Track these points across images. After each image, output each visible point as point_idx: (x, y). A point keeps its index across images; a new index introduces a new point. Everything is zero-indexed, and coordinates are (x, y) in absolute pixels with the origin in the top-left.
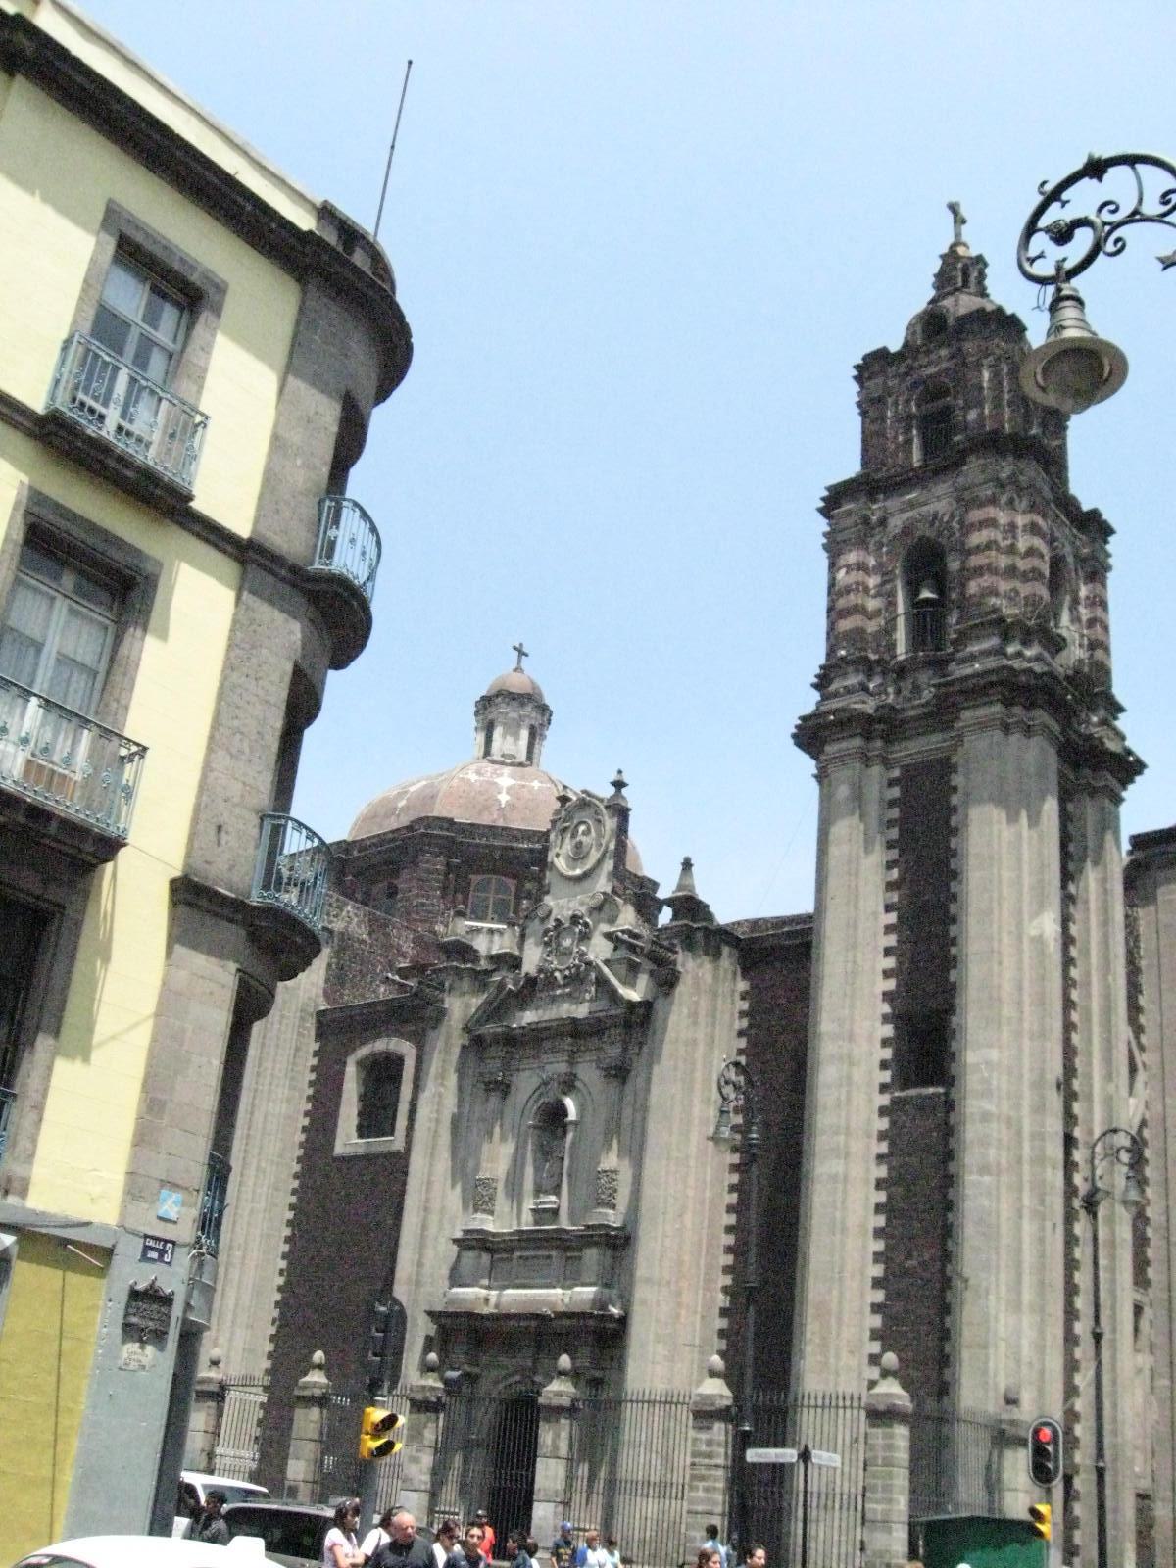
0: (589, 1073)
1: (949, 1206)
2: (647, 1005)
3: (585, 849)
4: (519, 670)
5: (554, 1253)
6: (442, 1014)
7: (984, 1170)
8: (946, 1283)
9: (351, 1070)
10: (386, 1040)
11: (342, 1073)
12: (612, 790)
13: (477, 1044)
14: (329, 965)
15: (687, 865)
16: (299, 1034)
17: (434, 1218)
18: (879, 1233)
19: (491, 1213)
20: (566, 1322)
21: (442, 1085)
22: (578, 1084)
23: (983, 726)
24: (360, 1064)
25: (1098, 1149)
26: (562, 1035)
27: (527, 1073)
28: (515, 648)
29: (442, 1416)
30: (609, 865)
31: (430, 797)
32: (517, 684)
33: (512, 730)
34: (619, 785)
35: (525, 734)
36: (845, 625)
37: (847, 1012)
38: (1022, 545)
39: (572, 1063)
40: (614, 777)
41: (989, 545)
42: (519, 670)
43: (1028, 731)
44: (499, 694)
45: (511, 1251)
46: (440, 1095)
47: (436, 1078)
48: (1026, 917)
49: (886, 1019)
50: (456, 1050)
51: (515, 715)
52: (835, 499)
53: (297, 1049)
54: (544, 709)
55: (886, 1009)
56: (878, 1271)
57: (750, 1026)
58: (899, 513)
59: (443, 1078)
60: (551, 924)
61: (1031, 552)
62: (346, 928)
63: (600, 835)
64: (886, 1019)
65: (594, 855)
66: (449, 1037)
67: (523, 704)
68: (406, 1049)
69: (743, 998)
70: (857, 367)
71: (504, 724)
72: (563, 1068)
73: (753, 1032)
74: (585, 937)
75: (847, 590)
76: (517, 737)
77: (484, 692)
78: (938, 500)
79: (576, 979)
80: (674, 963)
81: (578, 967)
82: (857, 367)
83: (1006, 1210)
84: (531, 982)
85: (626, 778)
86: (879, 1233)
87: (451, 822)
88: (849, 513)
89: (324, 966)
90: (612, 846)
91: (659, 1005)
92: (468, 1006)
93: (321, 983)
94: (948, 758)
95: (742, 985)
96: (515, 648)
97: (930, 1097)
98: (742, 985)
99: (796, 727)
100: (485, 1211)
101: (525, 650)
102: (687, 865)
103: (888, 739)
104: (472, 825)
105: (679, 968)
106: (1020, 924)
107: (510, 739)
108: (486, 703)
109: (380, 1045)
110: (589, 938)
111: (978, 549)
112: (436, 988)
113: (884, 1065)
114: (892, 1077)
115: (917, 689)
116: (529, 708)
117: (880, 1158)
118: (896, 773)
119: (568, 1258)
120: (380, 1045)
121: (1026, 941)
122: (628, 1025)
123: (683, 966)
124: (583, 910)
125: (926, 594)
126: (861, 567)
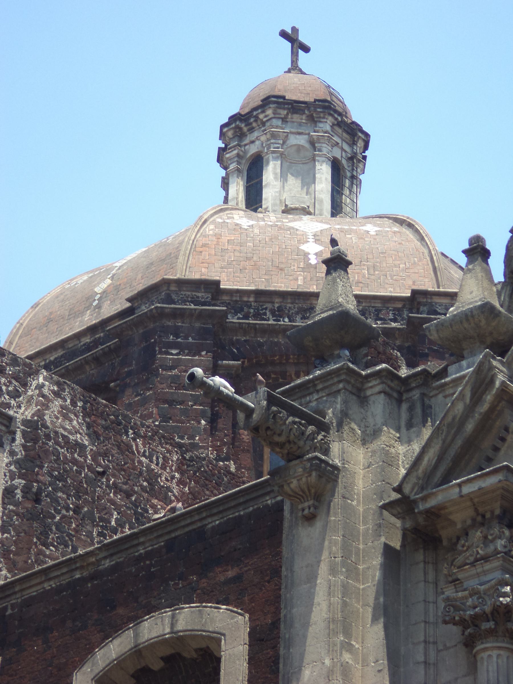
4: (295, 67)
6: (329, 475)
10: (168, 613)
21: (348, 647)
28: (284, 34)
31: (169, 254)
32: (295, 89)
33: (299, 166)
35: (324, 173)
42: (295, 67)
44: (266, 102)
47: (331, 633)
50: (373, 565)
51: (302, 141)
54: (355, 135)
59: (347, 632)
62: (40, 414)
66: (350, 535)
67: (313, 120)
68: (230, 628)
71: (282, 156)
76: (309, 180)
77: (235, 110)
87: (212, 287)
92: (389, 461)
96: (284, 34)
101: (302, 38)
104: (259, 293)
107: (294, 183)
108: (238, 127)
112: (311, 420)
116: (326, 125)
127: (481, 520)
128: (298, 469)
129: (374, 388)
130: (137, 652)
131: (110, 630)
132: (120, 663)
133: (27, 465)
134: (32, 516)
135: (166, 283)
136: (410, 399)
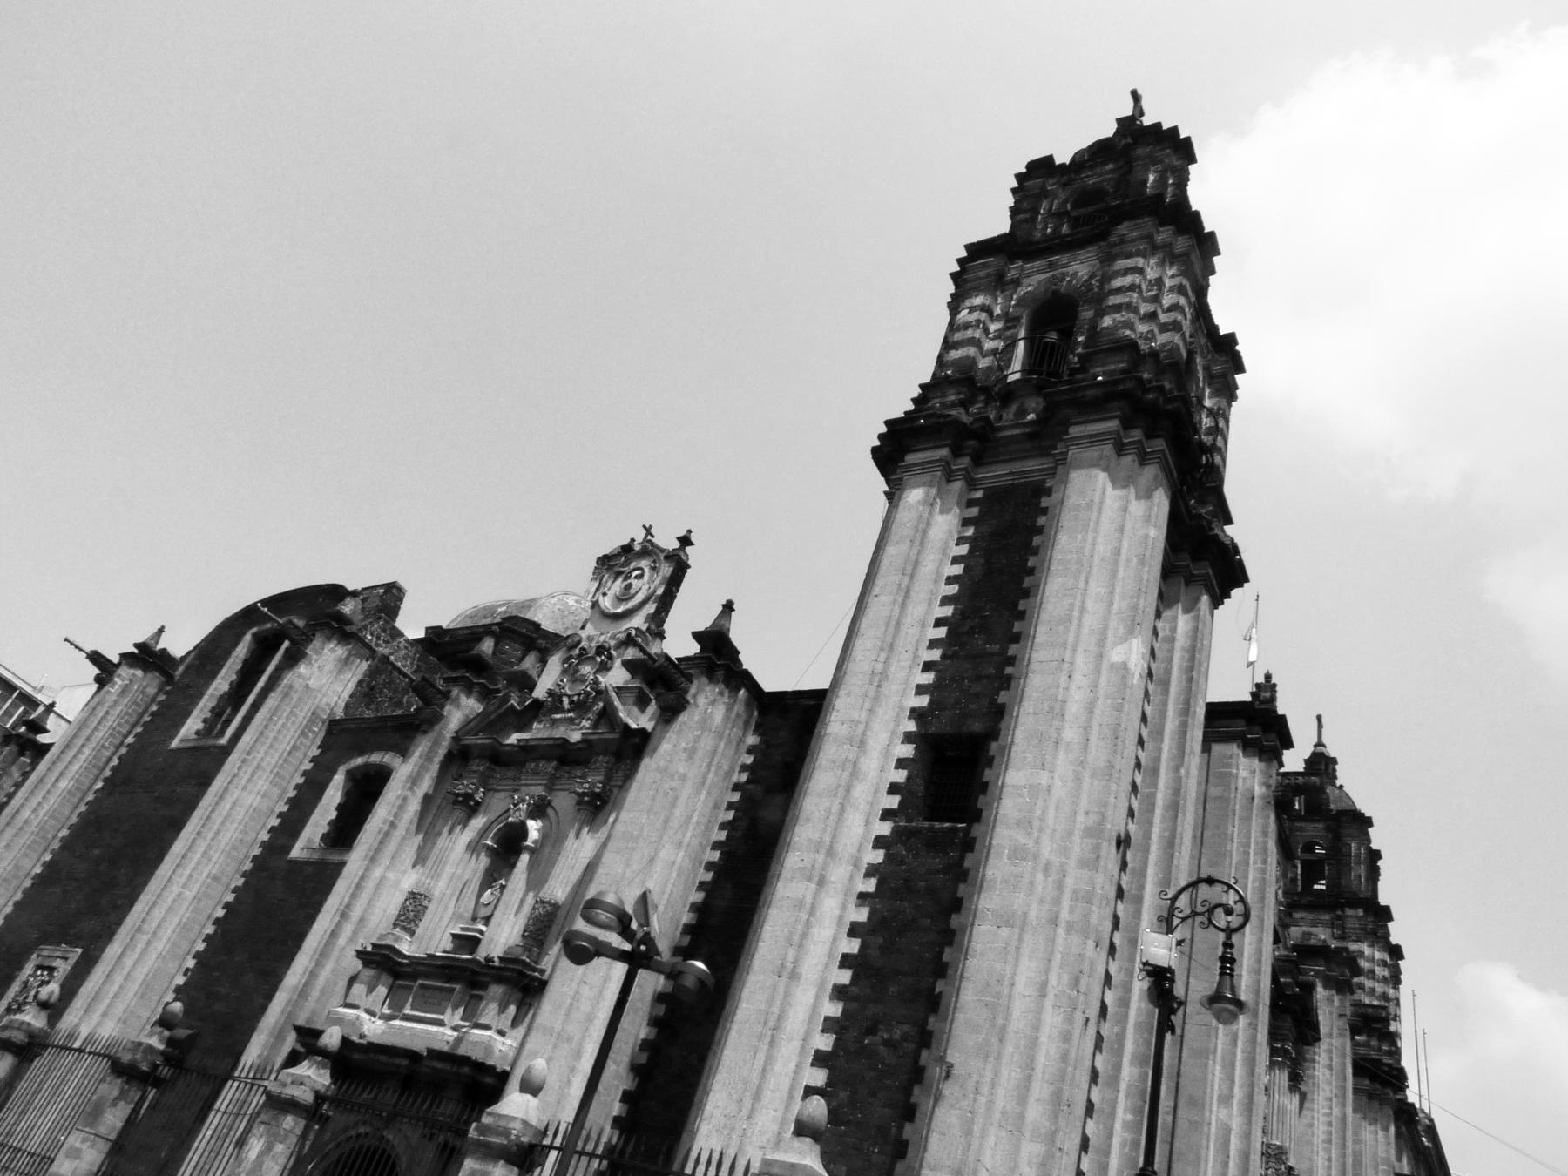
0: (563, 802)
1: (941, 970)
2: (644, 735)
3: (632, 591)
5: (458, 987)
7: (1005, 919)
8: (917, 1074)
9: (339, 779)
11: (329, 780)
12: (677, 545)
13: (458, 757)
14: (360, 683)
15: (728, 607)
17: (348, 928)
18: (839, 992)
19: (412, 933)
20: (439, 1065)
21: (411, 789)
22: (550, 811)
23: (1093, 439)
24: (350, 775)
25: (1183, 902)
26: (548, 758)
27: (502, 794)
29: (152, 1093)
30: (651, 608)
31: (528, 605)
34: (685, 541)
36: (954, 354)
37: (864, 715)
38: (1167, 300)
39: (550, 788)
40: (682, 533)
41: (1132, 288)
45: (414, 977)
46: (405, 799)
48: (1110, 639)
49: (908, 738)
52: (977, 251)
53: (295, 747)
55: (911, 726)
56: (825, 1043)
57: (748, 781)
58: (1033, 279)
60: (577, 651)
61: (1175, 307)
63: (651, 580)
64: (908, 738)
65: (640, 597)
66: (436, 743)
69: (749, 752)
70: (1019, 177)
72: (539, 791)
73: (750, 787)
74: (604, 668)
75: (967, 326)
77: (607, 552)
78: (1080, 267)
79: (581, 706)
80: (686, 691)
81: (587, 694)
82: (1019, 177)
83: (1027, 971)
84: (538, 704)
85: (693, 538)
86: (839, 992)
87: (537, 626)
88: (985, 265)
89: (355, 680)
90: (660, 592)
91: (657, 733)
93: (346, 695)
94: (1044, 481)
95: (752, 740)
97: (942, 830)
98: (752, 740)
99: (881, 437)
100: (404, 929)
102: (728, 607)
103: (979, 460)
105: (689, 697)
106: (1102, 643)
109: (375, 758)
110: (608, 669)
111: (1119, 291)
113: (893, 789)
114: (901, 803)
115: (1022, 412)
117: (863, 897)
118: (979, 494)
119: (472, 997)
120: (375, 758)
121: (1105, 665)
122: (619, 756)
123: (695, 697)
124: (612, 643)
125: (1053, 337)
126: (983, 308)
127: (481, 757)
128: (428, 711)
129: (476, 689)
130: (366, 765)
131: (361, 754)
132: (359, 767)
133: (372, 673)
134: (366, 695)
135: (516, 617)
136: (486, 695)
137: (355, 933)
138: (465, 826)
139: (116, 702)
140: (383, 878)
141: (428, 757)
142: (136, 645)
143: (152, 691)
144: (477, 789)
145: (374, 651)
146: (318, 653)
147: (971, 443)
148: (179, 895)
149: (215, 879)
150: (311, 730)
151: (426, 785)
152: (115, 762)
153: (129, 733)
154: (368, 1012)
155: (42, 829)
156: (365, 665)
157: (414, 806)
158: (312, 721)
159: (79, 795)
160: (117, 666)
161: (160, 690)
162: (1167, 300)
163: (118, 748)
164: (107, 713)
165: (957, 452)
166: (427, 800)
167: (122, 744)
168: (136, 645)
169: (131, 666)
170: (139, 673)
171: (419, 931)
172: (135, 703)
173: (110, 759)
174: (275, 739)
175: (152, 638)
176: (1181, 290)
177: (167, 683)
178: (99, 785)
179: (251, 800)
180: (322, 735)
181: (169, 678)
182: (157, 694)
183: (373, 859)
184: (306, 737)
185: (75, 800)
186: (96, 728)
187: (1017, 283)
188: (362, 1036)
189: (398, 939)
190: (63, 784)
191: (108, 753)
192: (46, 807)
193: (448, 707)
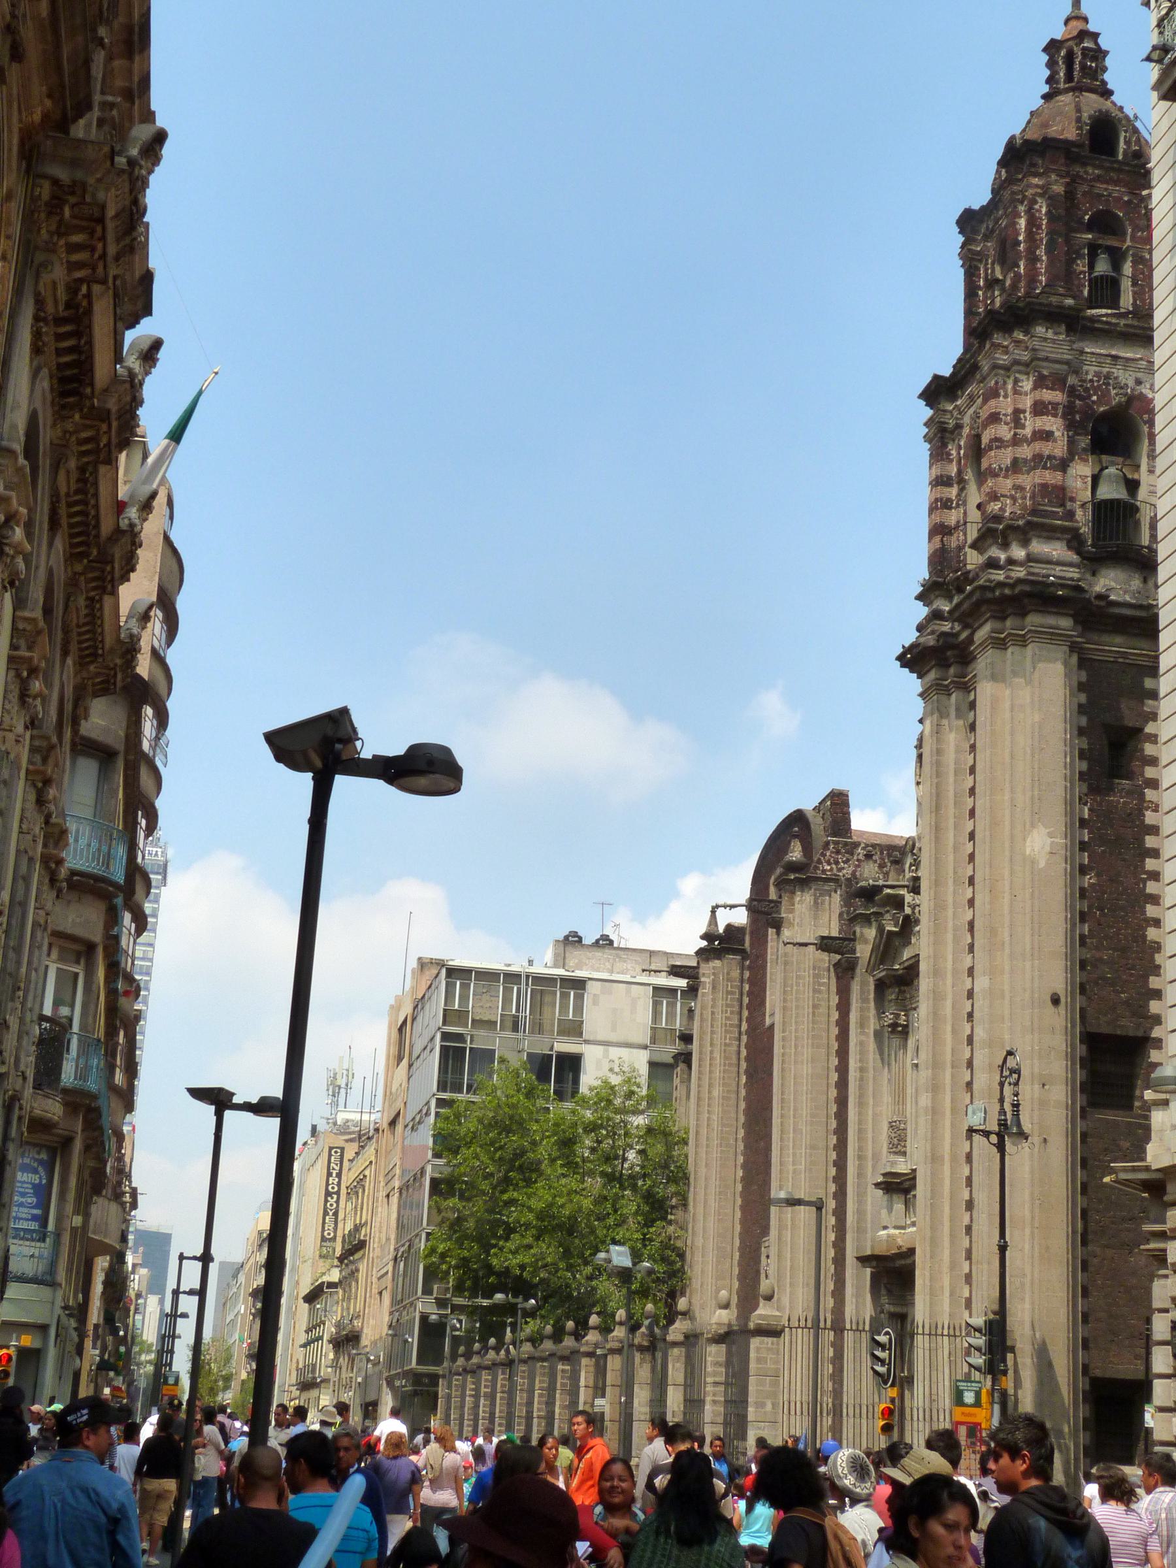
14: (841, 915)
16: (815, 991)
19: (904, 1154)
38: (1031, 424)
43: (1022, 642)
53: (815, 1006)
137: (874, 1167)
138: (905, 1046)
139: (714, 1000)
140: (875, 1115)
141: (865, 1000)
142: (703, 937)
143: (736, 973)
144: (897, 1016)
145: (835, 880)
146: (792, 911)
147: (949, 653)
148: (795, 1171)
149: (813, 1147)
150: (820, 984)
151: (872, 1025)
152: (744, 1052)
153: (740, 1020)
154: (896, 1227)
155: (722, 1138)
156: (837, 898)
157: (872, 1045)
158: (816, 976)
159: (733, 1096)
160: (697, 968)
161: (742, 969)
162: (1031, 424)
163: (739, 1040)
164: (713, 1013)
165: (944, 665)
166: (878, 1035)
167: (740, 1033)
168: (703, 937)
169: (707, 960)
170: (717, 963)
171: (908, 1150)
172: (728, 993)
173: (739, 1053)
174: (797, 1007)
175: (710, 924)
176: (1040, 409)
177: (744, 959)
178: (744, 1079)
179: (806, 1069)
180: (834, 981)
181: (742, 952)
182: (742, 974)
183: (861, 1104)
184: (819, 992)
185: (733, 1102)
186: (713, 1032)
187: (959, 427)
188: (900, 1247)
189: (893, 1163)
190: (715, 1093)
191: (735, 1048)
192: (715, 1117)
193: (858, 948)
